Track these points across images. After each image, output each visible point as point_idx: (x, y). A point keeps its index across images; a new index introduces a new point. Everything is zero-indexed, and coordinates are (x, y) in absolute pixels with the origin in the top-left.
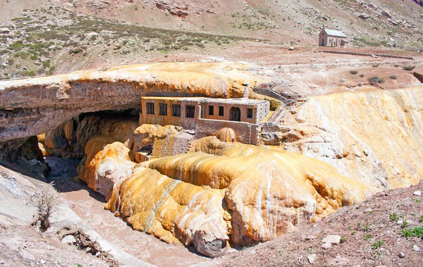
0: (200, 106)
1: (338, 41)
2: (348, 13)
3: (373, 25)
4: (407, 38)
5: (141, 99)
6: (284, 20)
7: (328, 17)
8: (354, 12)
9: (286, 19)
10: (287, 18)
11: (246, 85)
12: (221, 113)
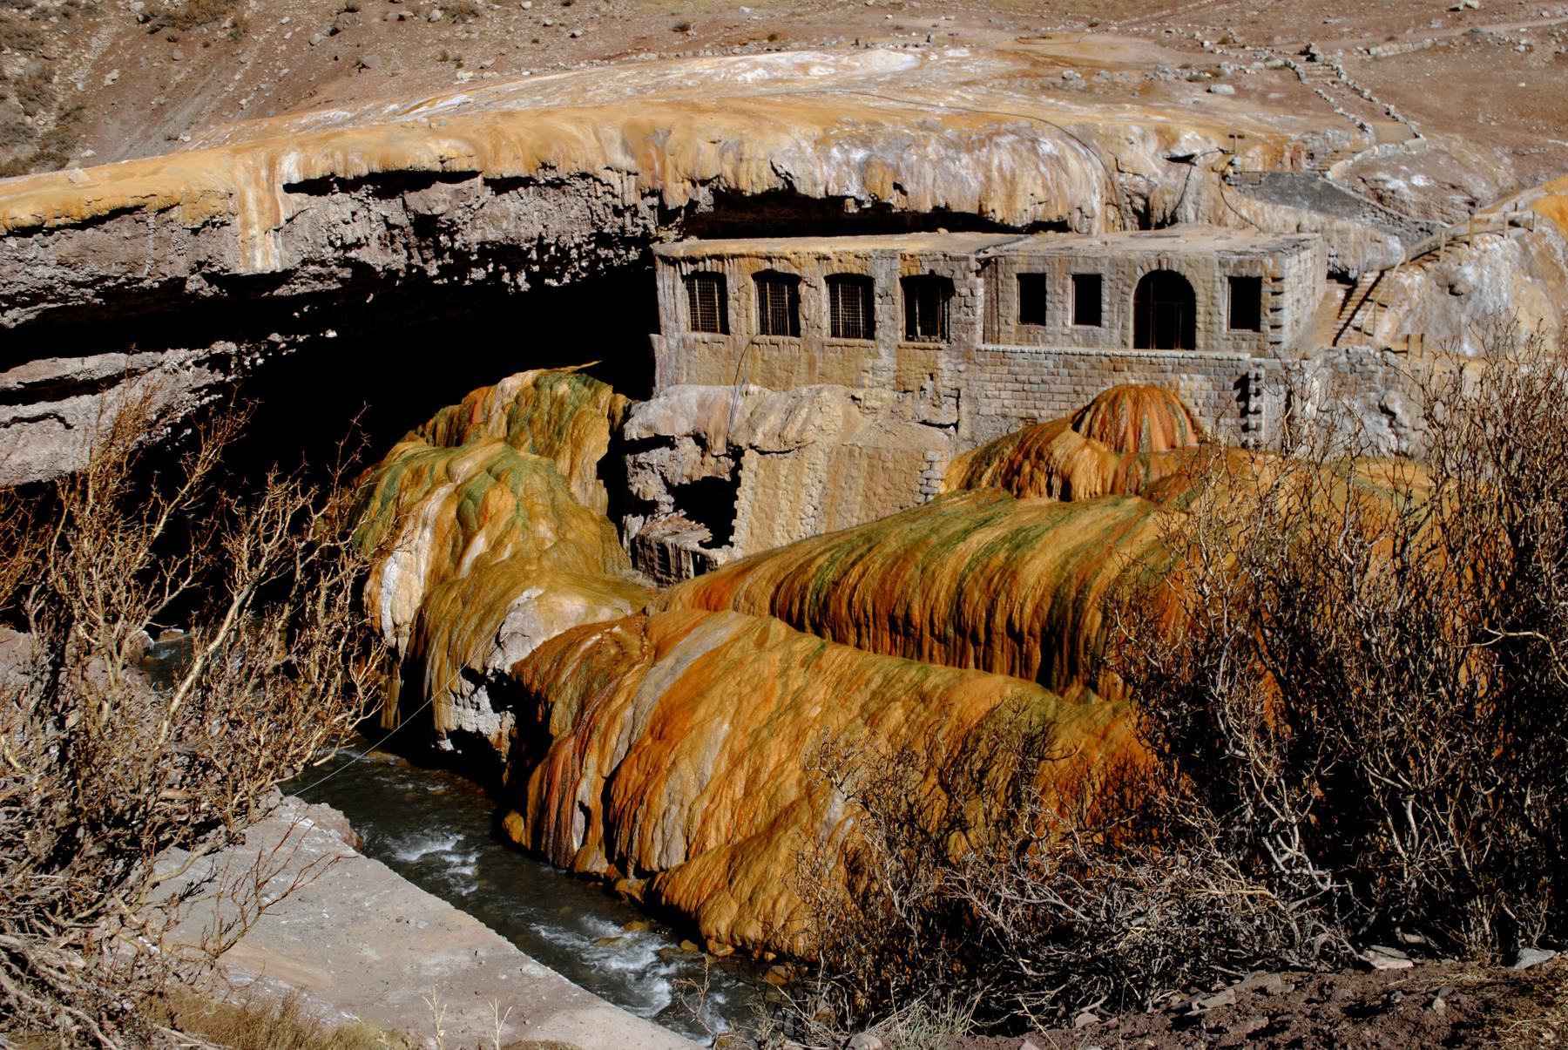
0: (980, 281)
5: (648, 257)
11: (1188, 159)
12: (1088, 310)
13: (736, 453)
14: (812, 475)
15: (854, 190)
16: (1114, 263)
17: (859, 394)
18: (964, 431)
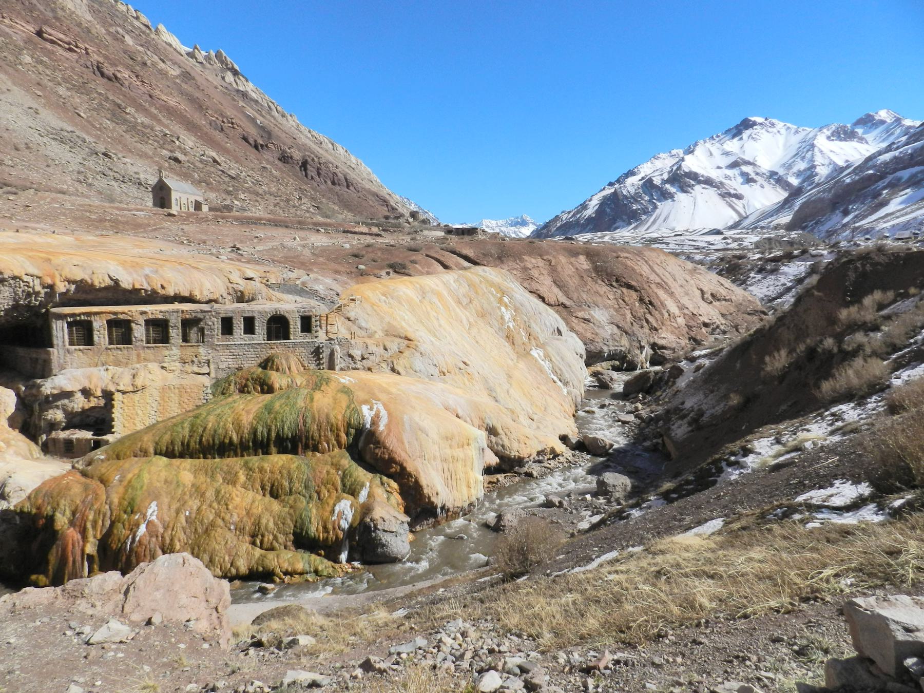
1: (190, 201)
2: (148, 149)
3: (199, 176)
4: (257, 201)
6: (17, 149)
7: (114, 154)
8: (159, 149)
9: (22, 146)
10: (22, 146)
13: (108, 396)
14: (151, 398)
15: (146, 286)
16: (260, 312)
17: (165, 365)
18: (213, 375)
